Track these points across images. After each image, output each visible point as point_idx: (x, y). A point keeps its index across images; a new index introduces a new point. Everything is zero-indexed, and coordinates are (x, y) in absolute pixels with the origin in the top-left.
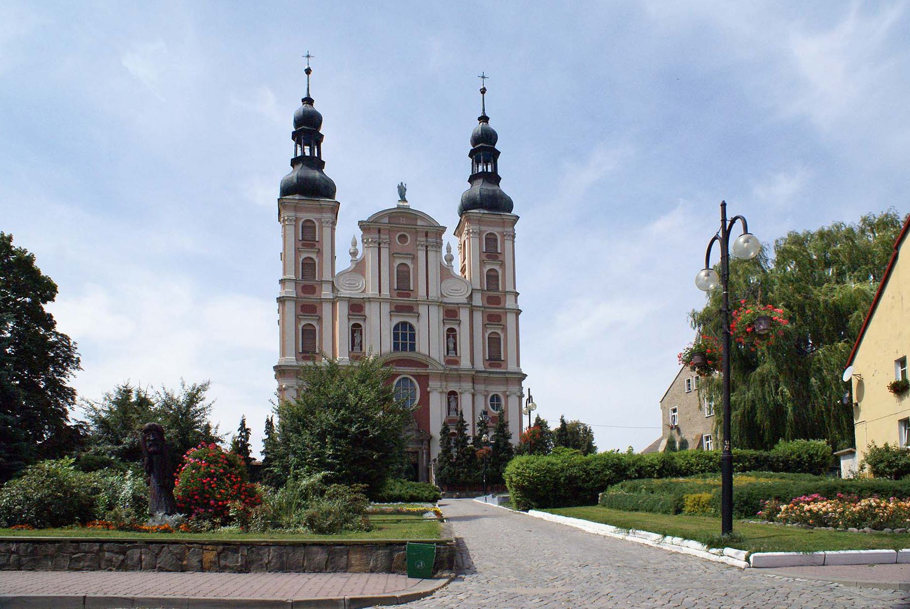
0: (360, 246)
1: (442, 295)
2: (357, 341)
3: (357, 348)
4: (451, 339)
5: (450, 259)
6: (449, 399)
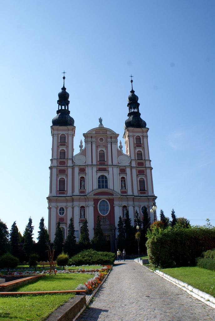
2: (83, 184)
3: (82, 188)
5: (121, 147)
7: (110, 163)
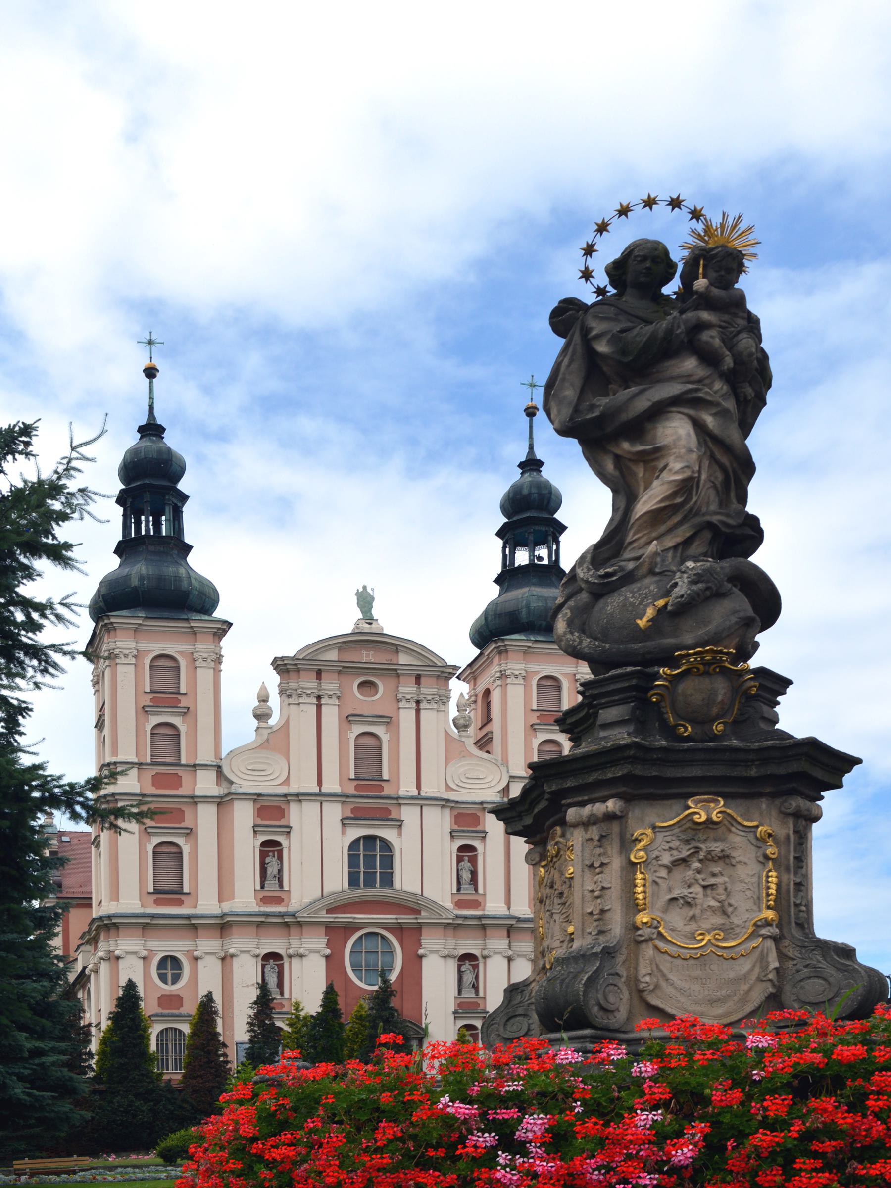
0: (275, 701)
2: (272, 870)
4: (466, 864)
6: (459, 967)
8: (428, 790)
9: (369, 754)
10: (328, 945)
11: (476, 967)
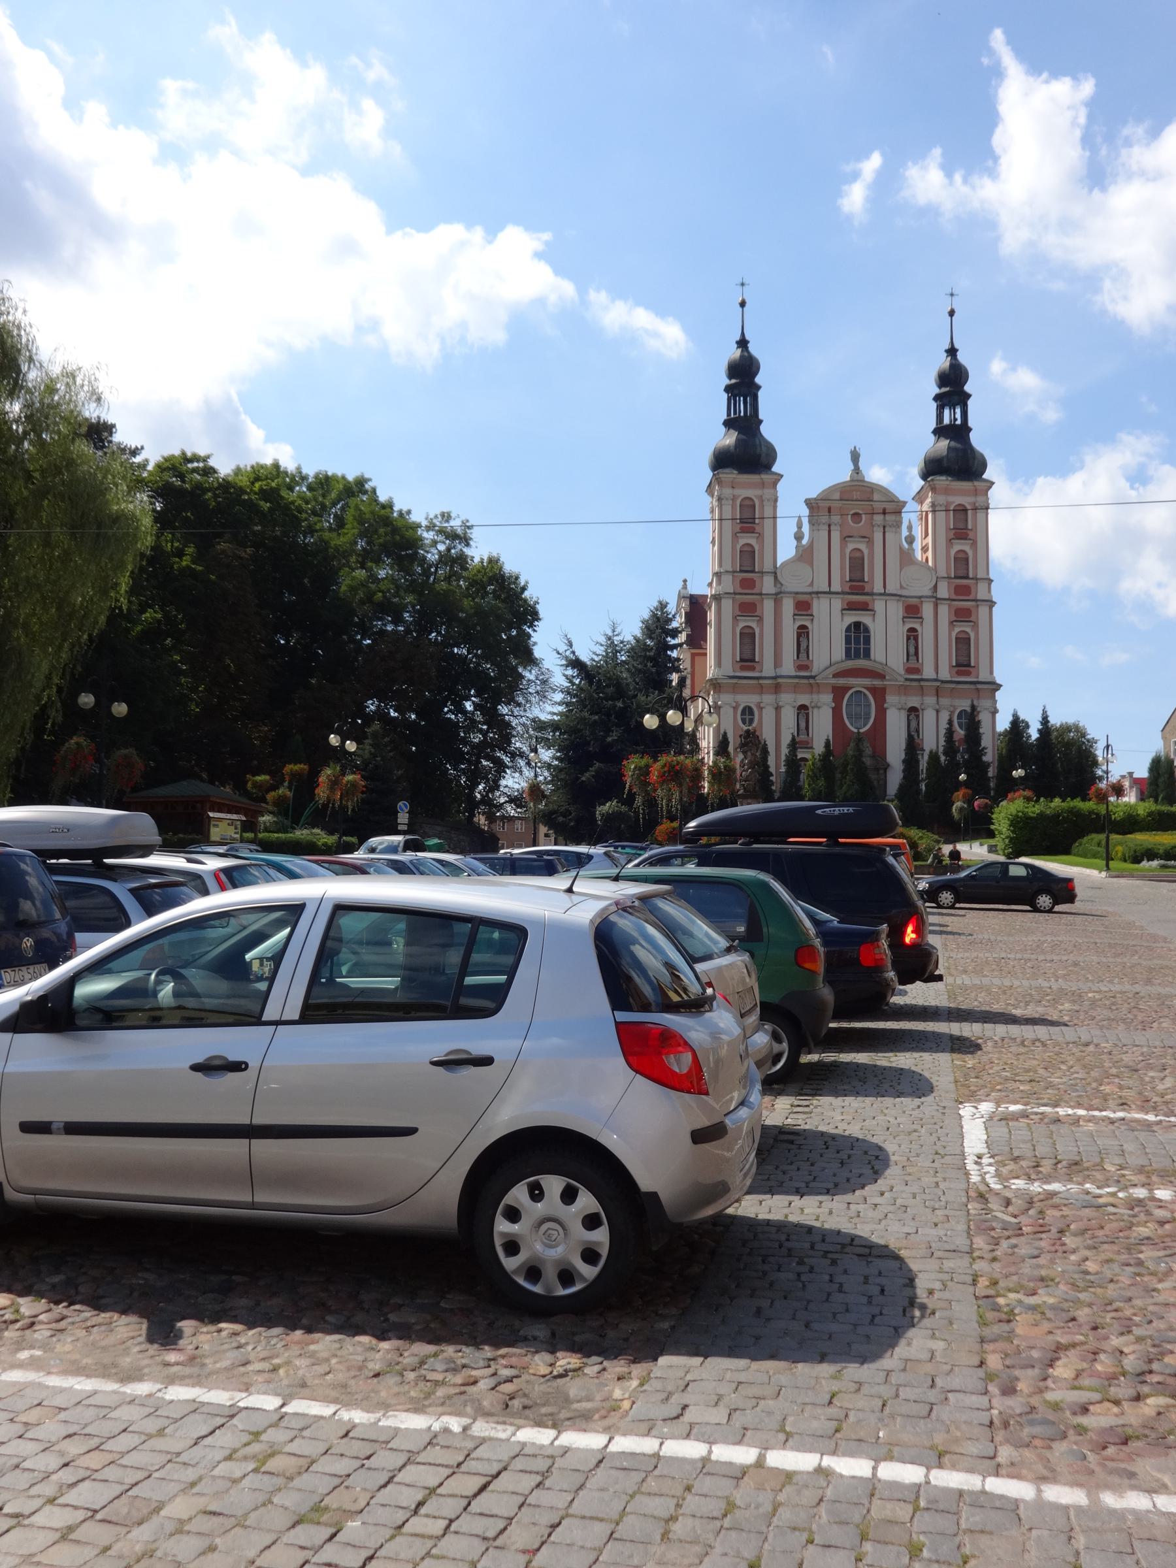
0: (806, 528)
1: (901, 587)
3: (803, 655)
4: (912, 641)
7: (878, 588)
8: (891, 588)
9: (857, 564)
10: (834, 700)
11: (918, 716)
